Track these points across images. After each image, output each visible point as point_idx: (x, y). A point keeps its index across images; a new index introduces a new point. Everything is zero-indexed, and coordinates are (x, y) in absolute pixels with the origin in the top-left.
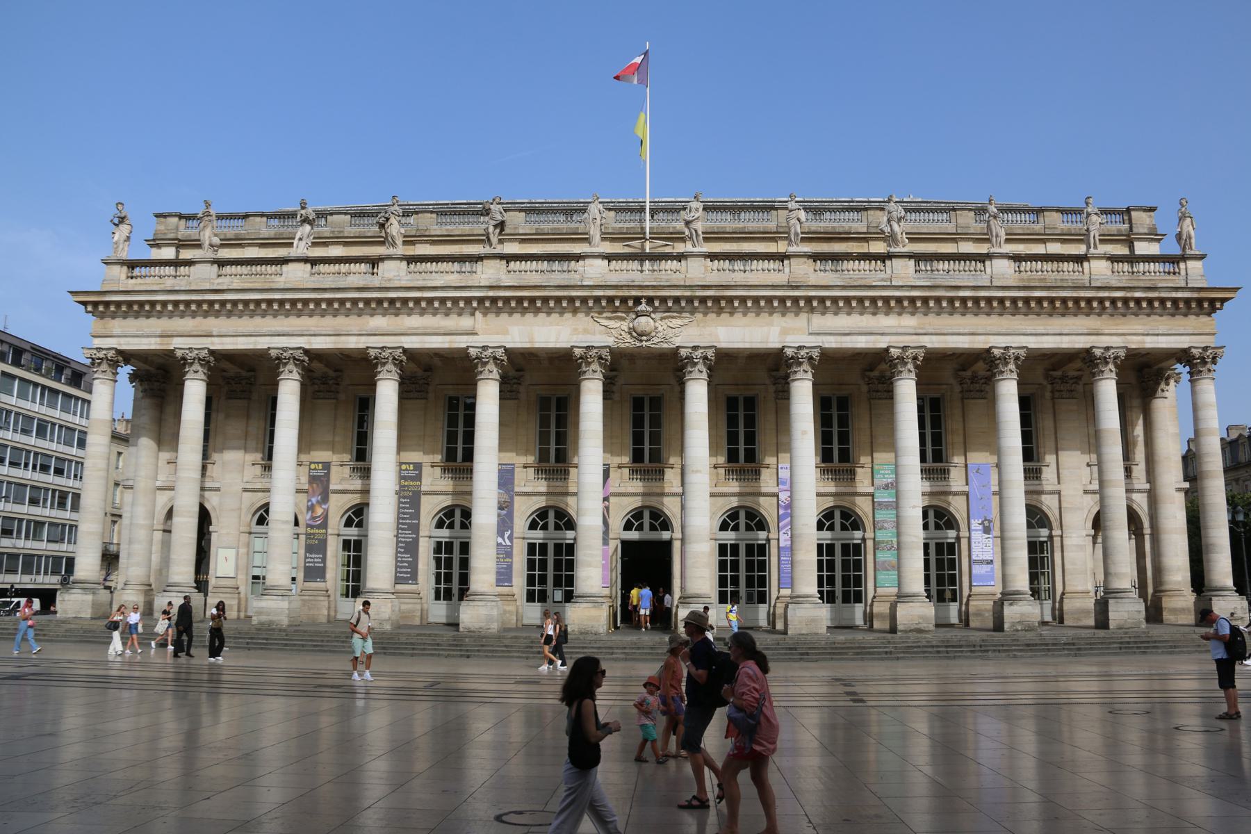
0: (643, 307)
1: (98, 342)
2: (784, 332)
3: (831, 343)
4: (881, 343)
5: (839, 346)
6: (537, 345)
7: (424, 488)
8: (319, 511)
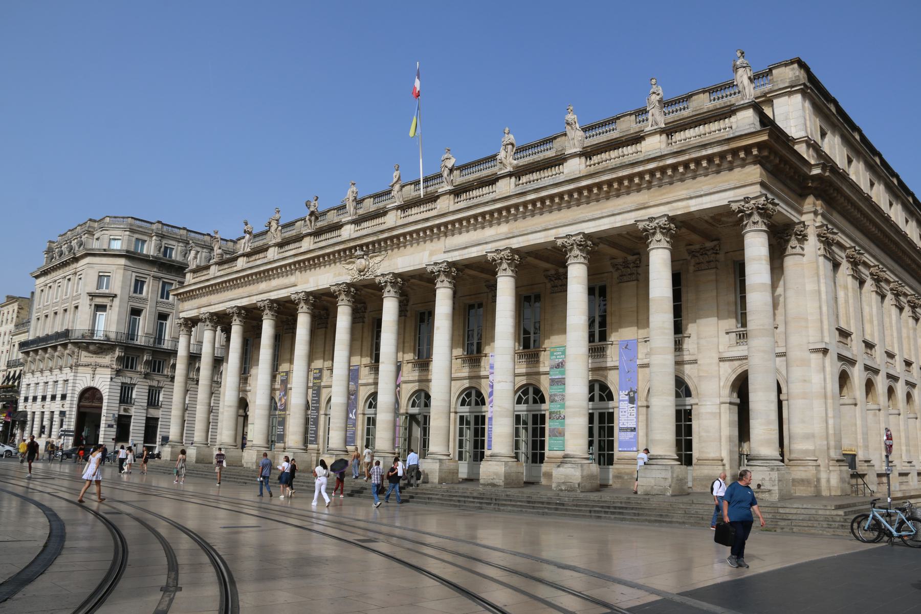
1: (182, 315)
2: (431, 254)
7: (323, 384)
8: (283, 401)
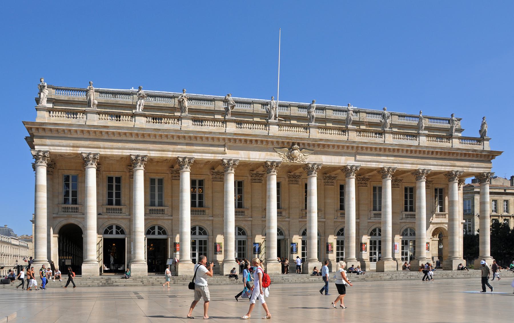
0: (296, 146)
2: (346, 160)
3: (363, 165)
4: (381, 165)
5: (366, 166)
6: (251, 160)
